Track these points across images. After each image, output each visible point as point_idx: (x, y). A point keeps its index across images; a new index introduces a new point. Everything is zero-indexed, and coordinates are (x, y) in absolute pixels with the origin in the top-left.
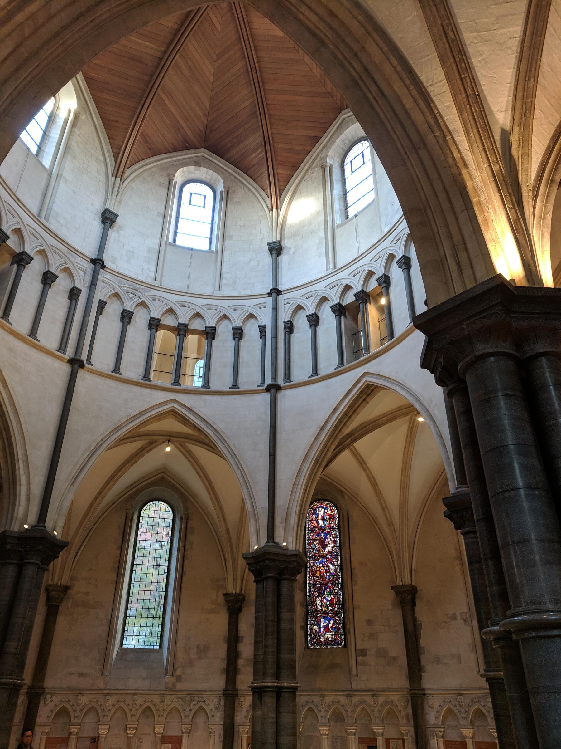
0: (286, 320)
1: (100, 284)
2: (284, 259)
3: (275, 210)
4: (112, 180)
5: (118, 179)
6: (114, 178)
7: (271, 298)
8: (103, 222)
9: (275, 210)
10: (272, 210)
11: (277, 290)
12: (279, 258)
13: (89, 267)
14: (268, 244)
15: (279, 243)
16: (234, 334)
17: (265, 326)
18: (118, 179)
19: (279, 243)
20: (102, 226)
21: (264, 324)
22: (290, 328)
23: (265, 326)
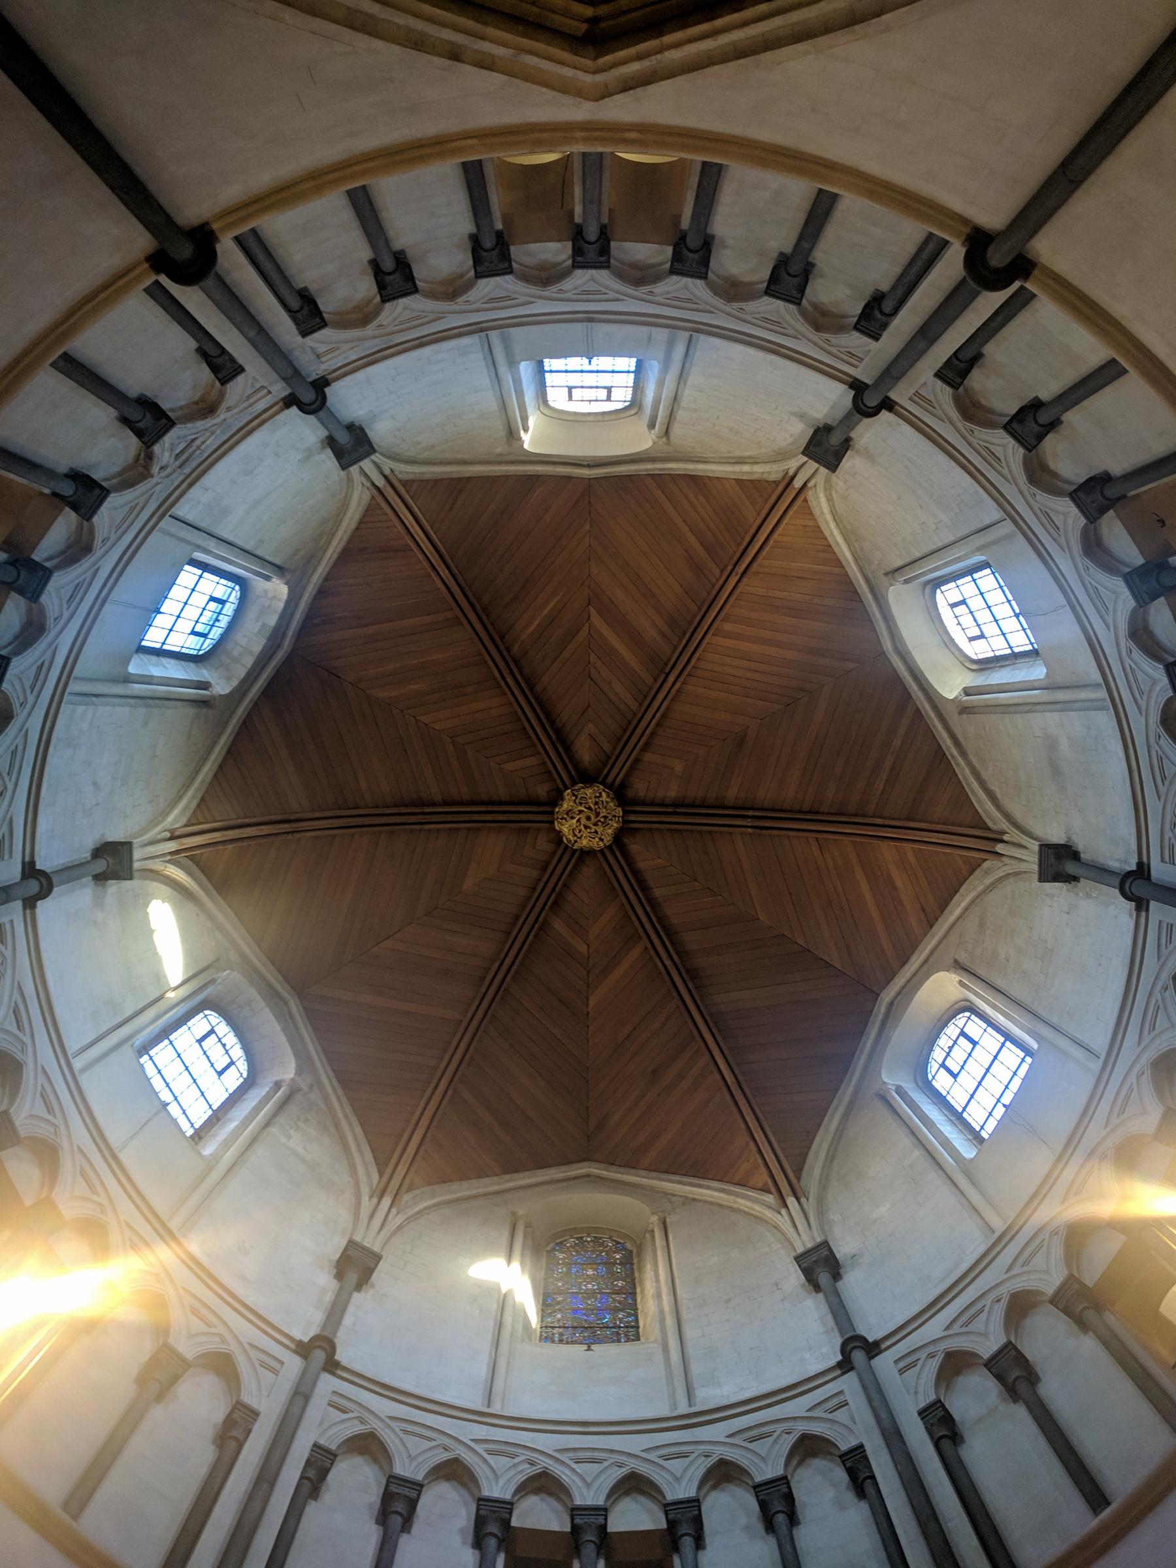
0: (922, 1405)
1: (317, 1409)
2: (853, 1283)
3: (791, 1201)
4: (367, 1204)
5: (387, 1201)
6: (375, 1200)
7: (851, 1376)
8: (339, 1275)
9: (791, 1201)
10: (786, 1206)
11: (864, 1339)
12: (840, 1285)
13: (293, 1365)
14: (798, 1259)
15: (825, 1244)
16: (763, 1505)
17: (861, 1446)
18: (387, 1201)
19: (825, 1244)
20: (334, 1284)
21: (854, 1443)
22: (942, 1425)
23: (860, 1448)
